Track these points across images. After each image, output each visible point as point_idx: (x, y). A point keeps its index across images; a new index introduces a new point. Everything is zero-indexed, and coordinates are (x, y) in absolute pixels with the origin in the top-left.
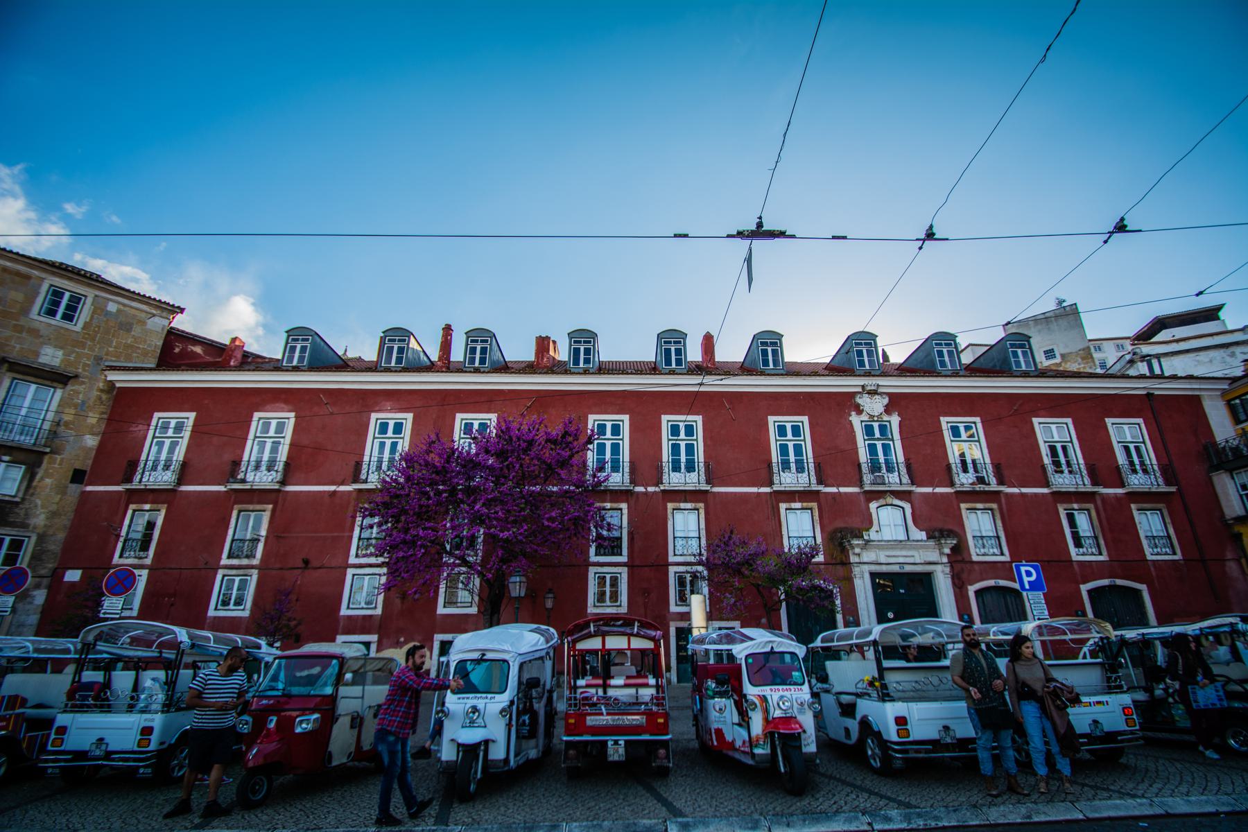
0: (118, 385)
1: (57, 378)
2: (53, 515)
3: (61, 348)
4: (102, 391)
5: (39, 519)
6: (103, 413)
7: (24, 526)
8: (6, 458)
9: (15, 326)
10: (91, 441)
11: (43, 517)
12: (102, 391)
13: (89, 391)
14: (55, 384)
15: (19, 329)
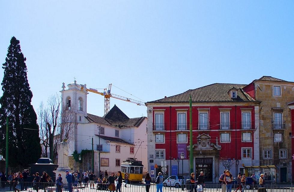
0: (291, 109)
1: (281, 111)
2: (289, 144)
3: (280, 102)
4: (289, 111)
5: (287, 146)
6: (290, 117)
7: (285, 148)
8: (278, 133)
9: (272, 99)
10: (290, 125)
11: (287, 145)
12: (289, 111)
13: (287, 112)
14: (281, 112)
15: (272, 100)
